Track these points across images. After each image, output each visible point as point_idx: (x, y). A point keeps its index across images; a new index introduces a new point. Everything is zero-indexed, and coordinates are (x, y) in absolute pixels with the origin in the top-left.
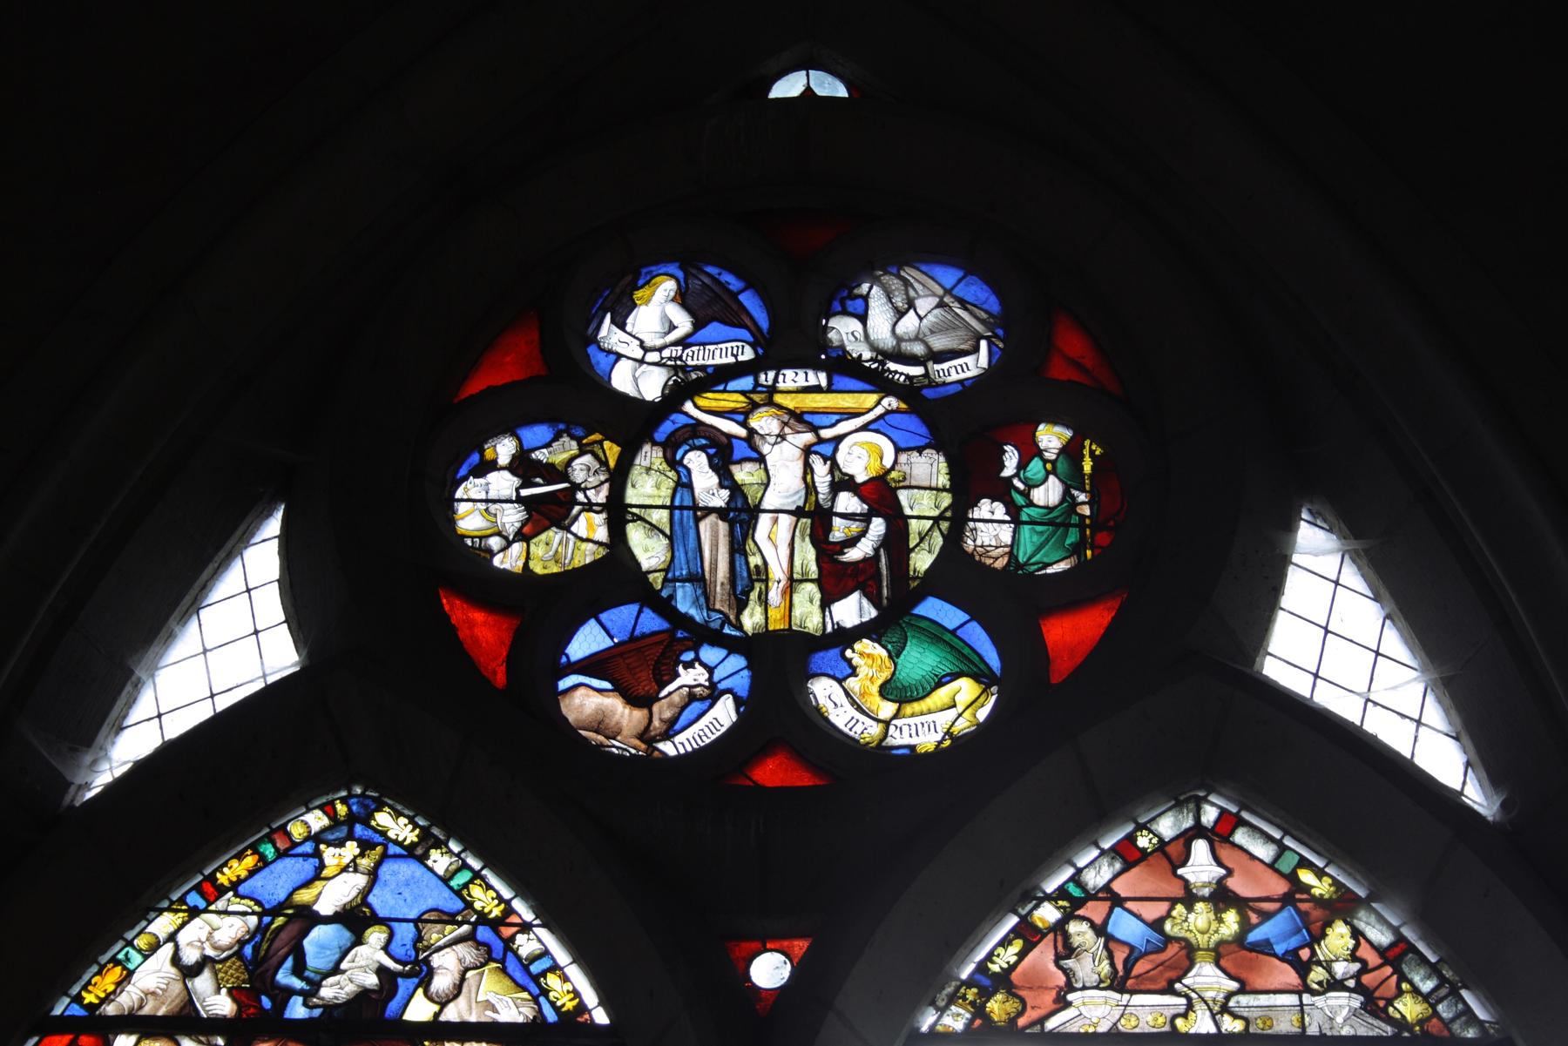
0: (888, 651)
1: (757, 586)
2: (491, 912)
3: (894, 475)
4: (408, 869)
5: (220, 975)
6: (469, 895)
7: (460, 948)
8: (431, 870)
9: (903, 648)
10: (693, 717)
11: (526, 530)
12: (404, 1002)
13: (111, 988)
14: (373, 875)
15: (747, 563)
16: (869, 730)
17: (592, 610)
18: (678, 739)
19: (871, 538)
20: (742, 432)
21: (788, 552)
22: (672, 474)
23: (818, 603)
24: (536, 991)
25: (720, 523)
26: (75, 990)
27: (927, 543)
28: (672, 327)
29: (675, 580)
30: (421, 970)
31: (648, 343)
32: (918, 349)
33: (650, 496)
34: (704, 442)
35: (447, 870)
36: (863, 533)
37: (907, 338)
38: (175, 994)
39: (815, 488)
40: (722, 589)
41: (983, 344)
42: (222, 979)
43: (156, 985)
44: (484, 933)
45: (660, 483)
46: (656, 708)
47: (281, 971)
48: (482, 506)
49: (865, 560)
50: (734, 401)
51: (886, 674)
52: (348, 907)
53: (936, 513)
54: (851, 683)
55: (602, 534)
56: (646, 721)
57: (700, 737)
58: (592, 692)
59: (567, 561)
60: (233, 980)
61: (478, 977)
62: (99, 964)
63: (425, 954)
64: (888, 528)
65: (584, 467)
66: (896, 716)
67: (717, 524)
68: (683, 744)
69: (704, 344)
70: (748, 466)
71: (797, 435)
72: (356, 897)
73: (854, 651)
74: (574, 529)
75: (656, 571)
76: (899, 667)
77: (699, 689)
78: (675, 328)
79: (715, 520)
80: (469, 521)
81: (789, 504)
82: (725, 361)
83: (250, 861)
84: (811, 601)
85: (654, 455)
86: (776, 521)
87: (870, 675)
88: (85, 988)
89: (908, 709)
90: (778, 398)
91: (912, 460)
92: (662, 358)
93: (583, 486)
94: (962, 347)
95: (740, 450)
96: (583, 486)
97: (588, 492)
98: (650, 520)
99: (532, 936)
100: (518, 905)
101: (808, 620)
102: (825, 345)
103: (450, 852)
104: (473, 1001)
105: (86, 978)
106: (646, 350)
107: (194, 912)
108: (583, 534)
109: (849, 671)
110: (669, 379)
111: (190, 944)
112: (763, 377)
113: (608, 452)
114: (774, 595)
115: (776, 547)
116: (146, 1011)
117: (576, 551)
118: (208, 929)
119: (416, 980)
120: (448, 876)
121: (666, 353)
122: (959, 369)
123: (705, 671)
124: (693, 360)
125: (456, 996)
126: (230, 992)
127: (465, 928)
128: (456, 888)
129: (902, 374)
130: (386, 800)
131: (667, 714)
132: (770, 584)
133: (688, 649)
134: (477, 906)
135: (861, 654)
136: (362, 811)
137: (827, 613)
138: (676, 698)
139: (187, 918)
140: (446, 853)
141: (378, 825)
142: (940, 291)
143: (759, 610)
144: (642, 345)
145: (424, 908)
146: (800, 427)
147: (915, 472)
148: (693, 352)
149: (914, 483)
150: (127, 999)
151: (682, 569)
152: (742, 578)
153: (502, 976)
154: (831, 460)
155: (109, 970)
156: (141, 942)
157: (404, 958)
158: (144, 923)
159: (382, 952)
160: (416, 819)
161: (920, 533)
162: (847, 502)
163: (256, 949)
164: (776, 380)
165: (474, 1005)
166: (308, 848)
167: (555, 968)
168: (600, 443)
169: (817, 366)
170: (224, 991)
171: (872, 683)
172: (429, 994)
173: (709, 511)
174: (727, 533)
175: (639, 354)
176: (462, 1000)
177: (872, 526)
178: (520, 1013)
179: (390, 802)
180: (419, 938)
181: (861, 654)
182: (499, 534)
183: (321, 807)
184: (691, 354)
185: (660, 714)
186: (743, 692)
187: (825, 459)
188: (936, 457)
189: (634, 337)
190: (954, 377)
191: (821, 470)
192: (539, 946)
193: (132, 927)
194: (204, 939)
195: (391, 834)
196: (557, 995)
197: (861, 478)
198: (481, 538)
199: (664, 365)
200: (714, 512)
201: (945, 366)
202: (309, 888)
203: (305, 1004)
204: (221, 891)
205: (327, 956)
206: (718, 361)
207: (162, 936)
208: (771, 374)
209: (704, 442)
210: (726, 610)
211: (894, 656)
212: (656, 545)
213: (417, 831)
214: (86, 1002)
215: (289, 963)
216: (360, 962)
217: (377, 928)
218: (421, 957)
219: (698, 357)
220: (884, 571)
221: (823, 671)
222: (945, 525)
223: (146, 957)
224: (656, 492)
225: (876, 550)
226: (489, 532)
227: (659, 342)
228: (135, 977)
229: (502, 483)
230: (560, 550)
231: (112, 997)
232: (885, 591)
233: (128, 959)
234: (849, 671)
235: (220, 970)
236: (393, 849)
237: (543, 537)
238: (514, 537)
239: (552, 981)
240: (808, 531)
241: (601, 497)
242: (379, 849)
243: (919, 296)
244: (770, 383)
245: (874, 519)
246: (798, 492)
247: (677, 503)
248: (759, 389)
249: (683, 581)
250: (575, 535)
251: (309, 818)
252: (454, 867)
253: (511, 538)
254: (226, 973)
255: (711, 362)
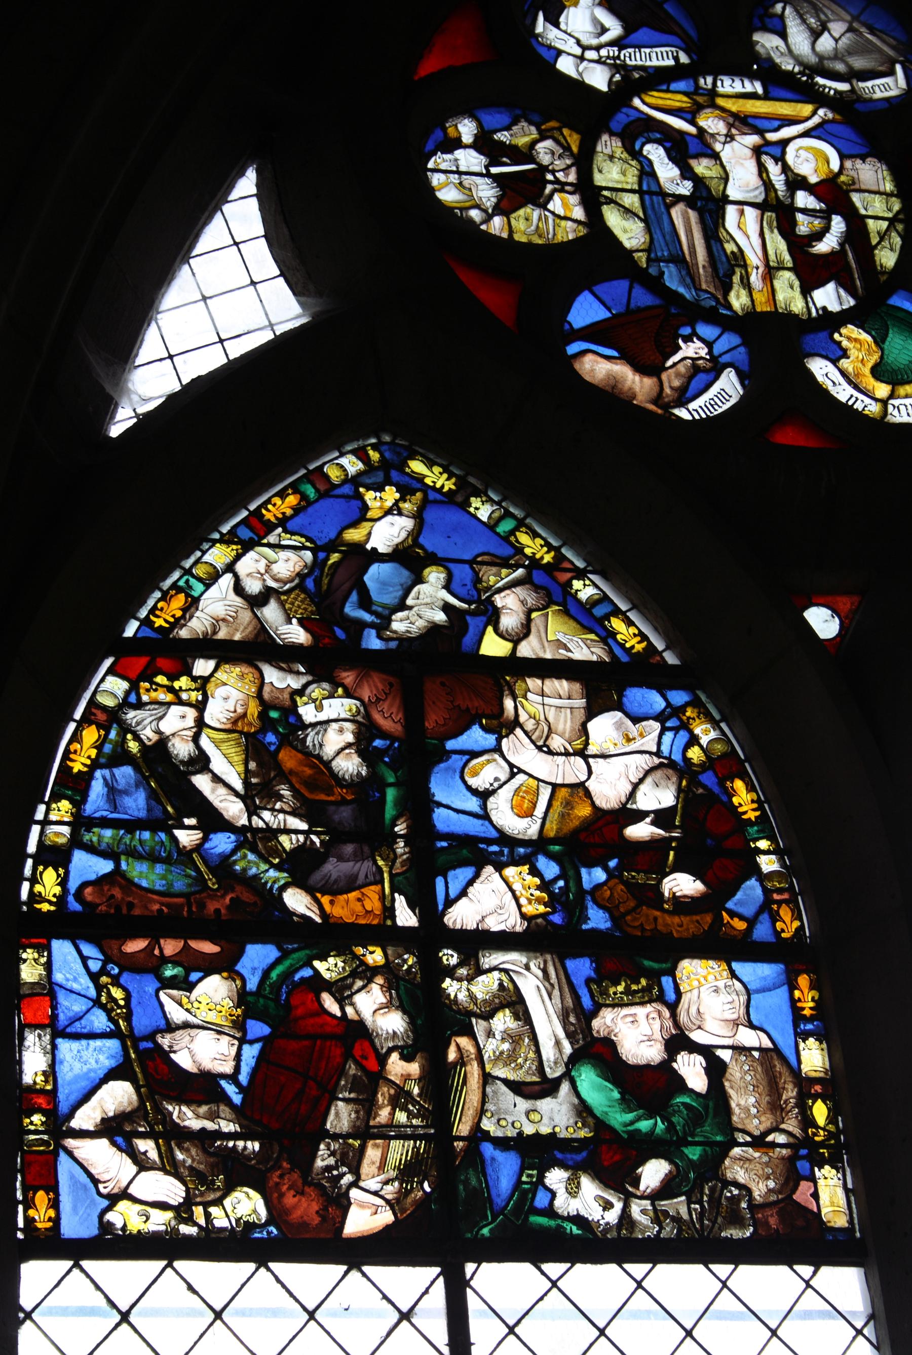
0: (873, 337)
1: (738, 271)
2: (542, 558)
3: (843, 178)
4: (452, 516)
5: (287, 606)
6: (517, 541)
7: (518, 590)
8: (475, 517)
9: (887, 335)
10: (702, 386)
11: (503, 205)
12: (478, 638)
13: (179, 614)
14: (418, 517)
15: (724, 250)
16: (869, 407)
17: (588, 283)
18: (693, 406)
19: (835, 234)
20: (692, 130)
21: (760, 241)
22: (634, 163)
23: (799, 289)
24: (603, 634)
25: (690, 211)
26: (143, 613)
27: (887, 242)
28: (604, 30)
29: (658, 260)
30: (487, 610)
31: (585, 41)
32: (840, 67)
33: (618, 182)
34: (658, 136)
35: (490, 517)
36: (826, 229)
37: (827, 56)
38: (246, 623)
39: (773, 186)
40: (705, 271)
41: (898, 68)
42: (290, 609)
43: (224, 612)
44: (538, 577)
45: (625, 171)
46: (664, 376)
47: (348, 605)
48: (454, 178)
49: (833, 253)
50: (679, 101)
51: (875, 357)
52: (400, 547)
53: (890, 215)
54: (844, 363)
55: (578, 213)
56: (656, 389)
57: (712, 406)
58: (599, 359)
59: (550, 236)
60: (300, 611)
61: (543, 618)
62: (161, 590)
63: (487, 595)
64: (847, 225)
65: (547, 151)
66: (892, 396)
67: (687, 212)
68: (696, 411)
69: (639, 47)
70: (705, 162)
71: (744, 136)
72: (407, 538)
73: (841, 335)
74: (550, 206)
75: (638, 251)
76: (886, 352)
77: (701, 362)
78: (607, 30)
79: (684, 207)
80: (448, 195)
81: (756, 197)
82: (661, 63)
83: (292, 500)
84: (792, 287)
85: (614, 144)
86: (742, 213)
87: (861, 357)
88: (152, 611)
89: (902, 391)
90: (720, 102)
91: (858, 166)
92: (601, 57)
93: (550, 168)
94: (880, 68)
95: (693, 146)
96: (550, 168)
97: (557, 174)
98: (622, 203)
99: (587, 582)
100: (567, 552)
101: (792, 305)
102: (756, 57)
103: (490, 500)
104: (545, 640)
105: (151, 603)
106: (585, 48)
107: (247, 546)
108: (560, 211)
109: (841, 353)
110: (612, 76)
111: (249, 575)
112: (702, 81)
113: (568, 139)
114: (755, 279)
115: (748, 237)
116: (222, 635)
117: (557, 228)
118: (263, 562)
119: (484, 619)
120: (492, 522)
121: (604, 52)
122: (882, 87)
123: (702, 345)
124: (631, 60)
125: (527, 634)
126: (301, 623)
127: (520, 572)
128: (502, 534)
129: (830, 88)
130: (417, 448)
131: (677, 383)
132: (749, 270)
133: (685, 325)
134: (528, 551)
135: (849, 339)
136: (395, 458)
137: (809, 299)
138: (681, 368)
139: (240, 551)
140: (487, 501)
141: (412, 471)
142: (848, 18)
143: (743, 293)
144: (578, 42)
145: (476, 552)
146: (746, 130)
147: (862, 177)
148: (630, 54)
149: (863, 187)
150: (198, 625)
151: (662, 251)
152: (722, 263)
153: (566, 619)
154: (780, 159)
155: (172, 596)
156: (200, 571)
157: (467, 597)
158: (199, 554)
159: (444, 591)
160: (451, 468)
161: (878, 233)
162: (803, 199)
163: (318, 582)
164: (714, 84)
165: (546, 644)
166: (347, 489)
167: (616, 612)
168: (559, 129)
169: (752, 77)
170: (294, 621)
171: (864, 365)
172: (500, 631)
173: (679, 198)
174: (698, 221)
175: (578, 51)
176: (532, 638)
177: (833, 223)
178: (592, 653)
179: (421, 450)
180: (477, 580)
181: (849, 339)
182: (477, 206)
183: (353, 452)
184: (627, 55)
185: (670, 382)
186: (745, 368)
187: (776, 161)
188: (879, 165)
189: (570, 35)
190: (879, 95)
191: (774, 170)
192: (595, 591)
193: (188, 557)
194: (263, 571)
195: (428, 481)
196: (624, 638)
197: (813, 179)
198: (461, 209)
199: (604, 63)
200: (683, 201)
201: (869, 84)
202: (356, 528)
203: (379, 637)
204: (270, 527)
205: (391, 592)
206: (655, 63)
207: (219, 566)
208: (710, 80)
209: (658, 136)
210: (712, 290)
211: (880, 341)
212: (634, 227)
213: (453, 480)
214: (156, 625)
215: (354, 597)
216: (424, 599)
217: (434, 568)
218: (483, 598)
219: (635, 58)
220: (852, 262)
221: (816, 351)
222: (900, 227)
223: (208, 586)
224: (623, 179)
225: (841, 245)
226: (467, 204)
227: (594, 42)
228: (202, 604)
229: (470, 159)
230: (540, 225)
231: (182, 622)
232: (858, 283)
233: (190, 587)
234: (841, 353)
235: (286, 601)
236: (432, 496)
237: (521, 212)
238: (493, 210)
239: (617, 624)
240: (775, 224)
241: (572, 177)
242: (419, 495)
243: (830, 21)
244: (710, 86)
245: (834, 216)
246: (757, 188)
247: (645, 188)
248: (701, 91)
249: (667, 261)
250: (553, 213)
251: (344, 461)
252: (496, 515)
253: (490, 211)
254: (293, 604)
255: (648, 63)
